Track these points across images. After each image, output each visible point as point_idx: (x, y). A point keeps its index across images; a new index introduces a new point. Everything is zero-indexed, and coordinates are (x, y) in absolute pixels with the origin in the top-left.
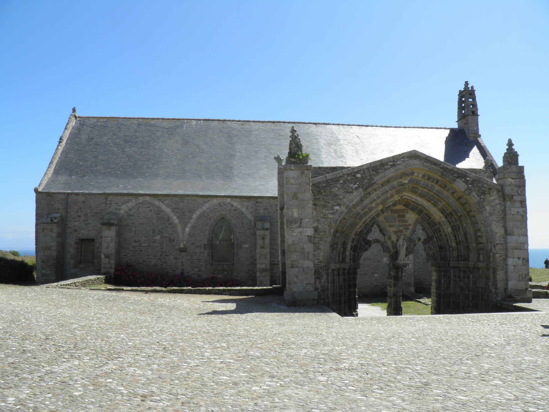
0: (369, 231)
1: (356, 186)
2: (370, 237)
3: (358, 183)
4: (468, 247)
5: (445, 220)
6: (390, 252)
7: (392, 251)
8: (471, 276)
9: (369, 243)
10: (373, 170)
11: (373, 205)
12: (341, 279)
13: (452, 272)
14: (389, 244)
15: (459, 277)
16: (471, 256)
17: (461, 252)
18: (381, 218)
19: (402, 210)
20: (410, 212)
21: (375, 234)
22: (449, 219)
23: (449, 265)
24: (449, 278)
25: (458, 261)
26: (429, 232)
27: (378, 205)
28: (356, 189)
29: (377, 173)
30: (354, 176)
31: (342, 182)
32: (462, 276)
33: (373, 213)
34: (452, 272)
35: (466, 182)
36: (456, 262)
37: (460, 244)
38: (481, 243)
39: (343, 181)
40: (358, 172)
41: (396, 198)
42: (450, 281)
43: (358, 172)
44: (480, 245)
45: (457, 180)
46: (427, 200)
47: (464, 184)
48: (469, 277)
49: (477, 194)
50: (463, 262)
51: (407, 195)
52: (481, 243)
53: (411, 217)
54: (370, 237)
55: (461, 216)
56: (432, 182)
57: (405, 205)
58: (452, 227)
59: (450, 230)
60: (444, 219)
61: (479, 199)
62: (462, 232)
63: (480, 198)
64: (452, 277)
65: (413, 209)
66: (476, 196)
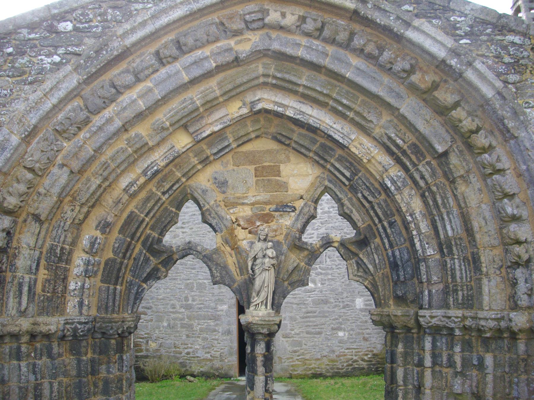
0: (167, 221)
1: (57, 59)
2: (172, 239)
3: (61, 51)
4: (475, 262)
5: (402, 173)
6: (234, 281)
7: (239, 278)
8: (489, 360)
9: (169, 259)
10: (114, 8)
11: (142, 130)
12: (24, 369)
13: (428, 345)
14: (231, 261)
15: (451, 364)
16: (486, 289)
17: (453, 277)
18: (203, 180)
19: (269, 152)
20: (293, 157)
21: (187, 228)
22: (412, 170)
23: (417, 322)
24: (420, 364)
25: (448, 307)
26: (356, 216)
27: (164, 133)
28: (57, 66)
29: (129, 15)
30: (52, 29)
31: (10, 50)
32: (458, 359)
33: (158, 158)
34: (428, 345)
35: (451, 30)
36: (439, 313)
37: (451, 252)
38: (519, 242)
39: (16, 47)
40: (62, 17)
41: (236, 109)
42: (423, 372)
43: (62, 17)
44: (517, 249)
45: (416, 22)
46: (335, 111)
47: (441, 37)
48: (481, 366)
49: (490, 68)
50: (459, 313)
51: (268, 99)
52: (519, 242)
53: (299, 176)
54: (172, 239)
55: (445, 154)
56: (332, 41)
57: (275, 138)
58: (423, 196)
59: (417, 205)
60: (395, 172)
61: (499, 84)
62: (455, 211)
63: (506, 82)
64: (428, 362)
65: (301, 151)
66: (490, 75)
